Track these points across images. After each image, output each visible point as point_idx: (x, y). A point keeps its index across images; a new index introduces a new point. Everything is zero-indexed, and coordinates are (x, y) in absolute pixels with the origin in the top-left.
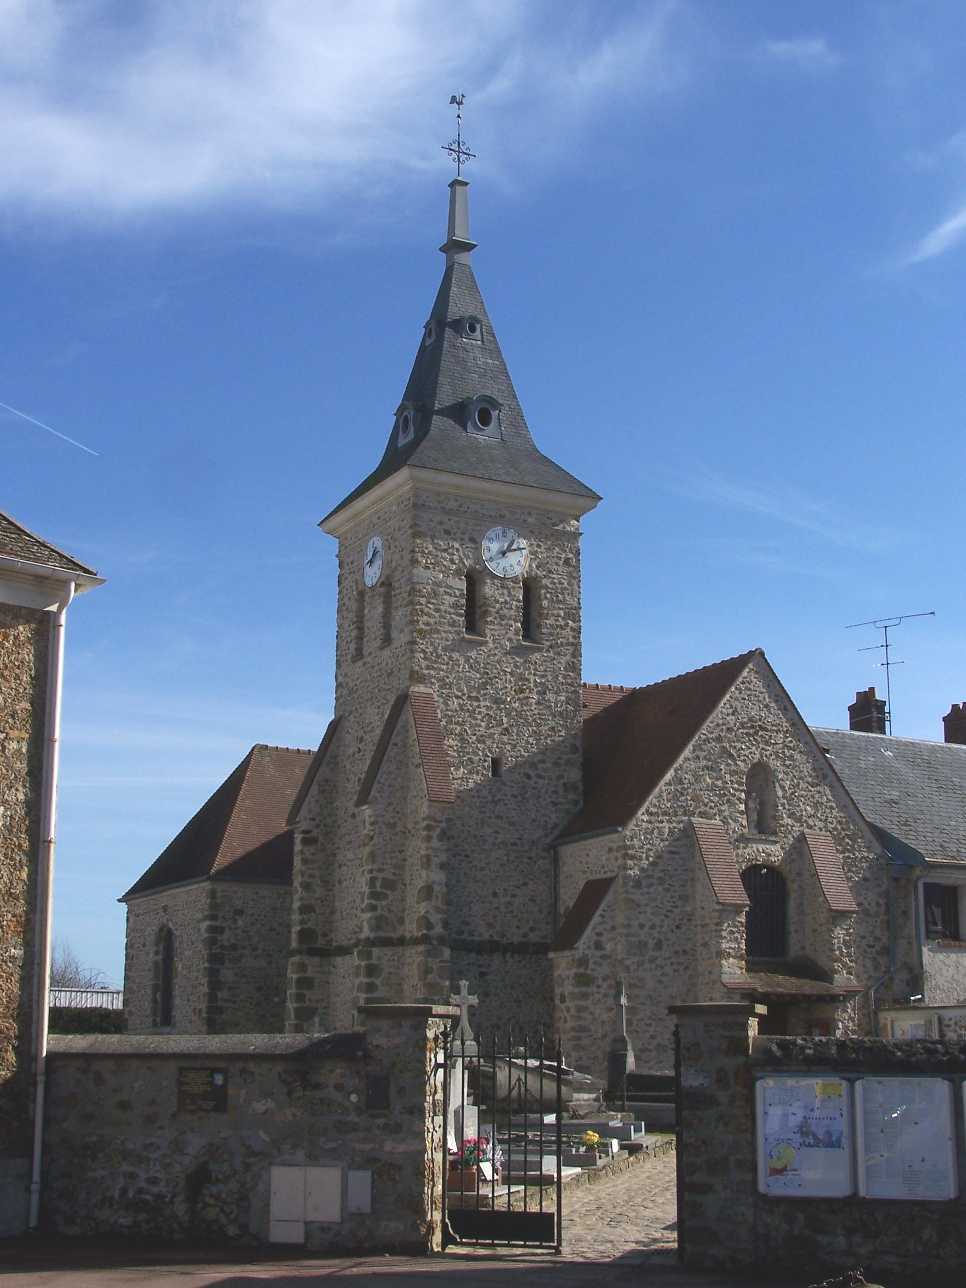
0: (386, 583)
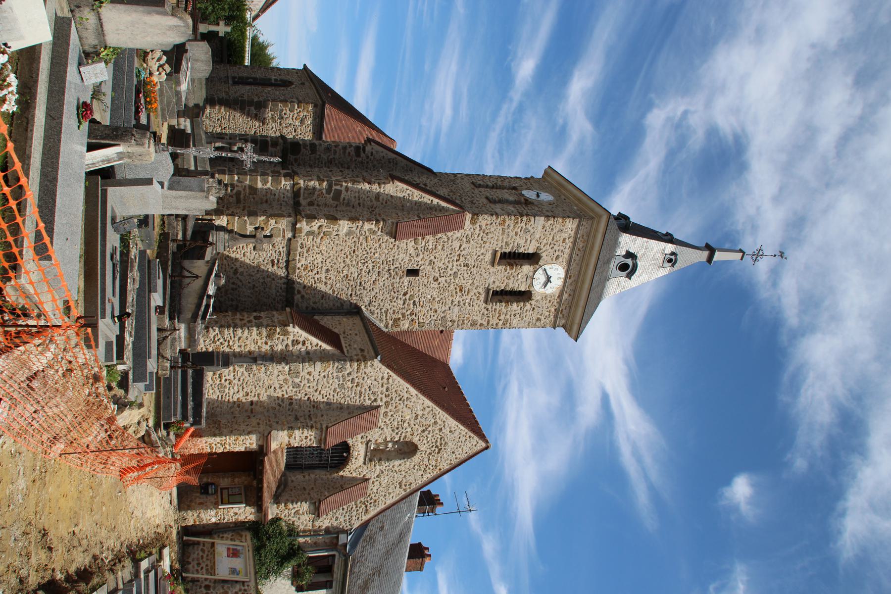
0: (527, 202)
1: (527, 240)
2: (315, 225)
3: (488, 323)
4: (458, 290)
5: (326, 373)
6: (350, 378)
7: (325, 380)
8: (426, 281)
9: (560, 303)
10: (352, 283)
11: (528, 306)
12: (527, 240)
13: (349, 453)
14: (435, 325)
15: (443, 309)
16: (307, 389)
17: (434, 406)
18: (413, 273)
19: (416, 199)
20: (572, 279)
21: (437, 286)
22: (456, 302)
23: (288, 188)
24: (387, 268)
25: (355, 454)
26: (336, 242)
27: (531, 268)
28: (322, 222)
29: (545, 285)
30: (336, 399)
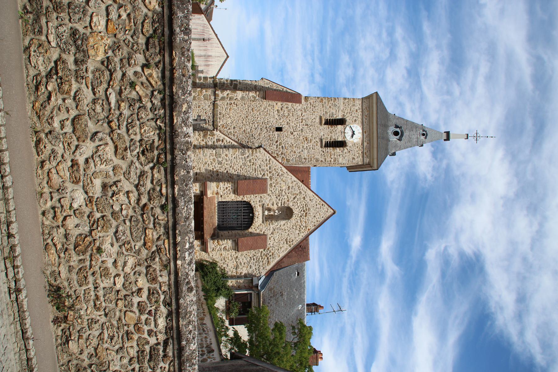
2: (226, 93)
5: (235, 156)
6: (249, 159)
8: (287, 134)
9: (363, 148)
10: (248, 135)
11: (346, 150)
13: (253, 214)
14: (296, 161)
15: (299, 151)
17: (298, 181)
18: (279, 129)
19: (275, 88)
20: (367, 133)
21: (293, 137)
25: (256, 213)
28: (228, 92)
29: (352, 136)
30: (243, 172)
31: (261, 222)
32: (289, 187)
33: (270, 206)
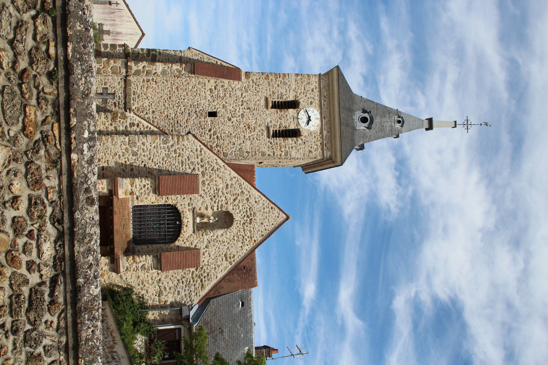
1: (286, 90)
2: (141, 65)
3: (274, 154)
4: (247, 127)
5: (155, 145)
6: (173, 149)
7: (155, 150)
8: (223, 120)
9: (322, 138)
10: (171, 121)
11: (300, 141)
12: (286, 90)
13: (180, 221)
14: (235, 155)
15: (239, 142)
16: (143, 157)
17: (239, 177)
18: (213, 114)
19: (206, 61)
20: (326, 119)
21: (231, 124)
22: (247, 137)
23: (121, 51)
24: (194, 110)
25: (185, 220)
26: (157, 91)
27: (295, 111)
28: (145, 63)
30: (165, 166)
31: (191, 232)
32: (227, 185)
33: (203, 211)
